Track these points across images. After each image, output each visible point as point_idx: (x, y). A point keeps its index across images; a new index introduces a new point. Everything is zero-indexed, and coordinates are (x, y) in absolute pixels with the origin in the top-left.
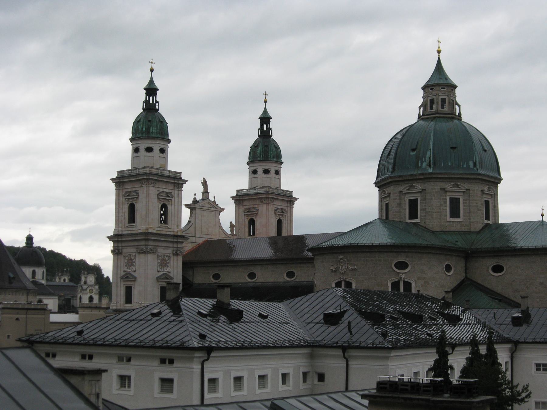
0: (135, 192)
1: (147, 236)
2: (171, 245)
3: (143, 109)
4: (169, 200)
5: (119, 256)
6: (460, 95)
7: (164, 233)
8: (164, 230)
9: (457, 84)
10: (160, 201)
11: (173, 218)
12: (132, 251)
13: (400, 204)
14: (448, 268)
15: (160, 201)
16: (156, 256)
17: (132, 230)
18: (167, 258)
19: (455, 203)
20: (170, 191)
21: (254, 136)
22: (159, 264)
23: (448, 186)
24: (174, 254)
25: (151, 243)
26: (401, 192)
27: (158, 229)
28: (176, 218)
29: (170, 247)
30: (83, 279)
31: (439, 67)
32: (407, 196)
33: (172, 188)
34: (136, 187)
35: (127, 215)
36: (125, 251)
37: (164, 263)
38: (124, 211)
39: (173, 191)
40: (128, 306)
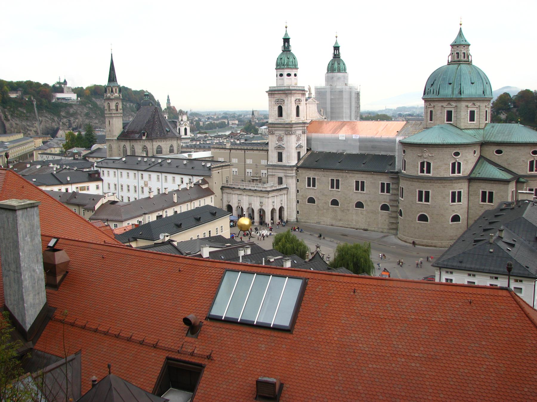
0: (282, 99)
1: (290, 125)
2: (301, 128)
3: (283, 51)
6: (472, 50)
7: (298, 122)
9: (470, 43)
12: (282, 133)
13: (441, 113)
14: (475, 152)
19: (472, 114)
21: (331, 57)
23: (470, 104)
24: (303, 133)
25: (293, 129)
26: (442, 106)
30: (180, 118)
31: (460, 33)
32: (446, 108)
33: (301, 96)
34: (283, 97)
35: (277, 112)
36: (276, 132)
37: (298, 139)
40: (280, 163)
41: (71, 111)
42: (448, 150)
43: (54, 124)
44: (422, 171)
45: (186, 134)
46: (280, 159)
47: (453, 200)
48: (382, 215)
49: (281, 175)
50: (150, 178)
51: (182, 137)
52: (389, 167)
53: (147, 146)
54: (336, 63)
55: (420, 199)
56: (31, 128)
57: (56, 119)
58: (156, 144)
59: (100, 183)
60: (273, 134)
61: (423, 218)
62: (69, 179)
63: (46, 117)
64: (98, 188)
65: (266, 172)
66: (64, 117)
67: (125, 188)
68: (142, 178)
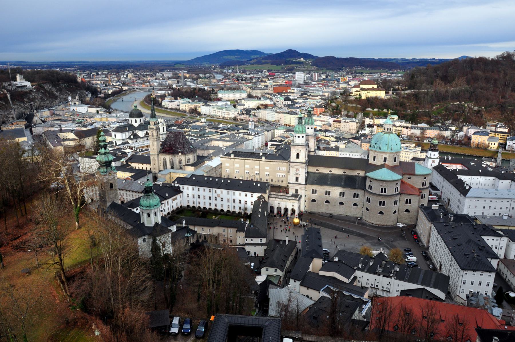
12: (299, 167)
17: (298, 160)
36: (295, 166)
40: (297, 182)
41: (31, 96)
42: (394, 182)
43: (22, 109)
44: (382, 192)
45: (164, 131)
46: (297, 179)
47: (395, 205)
48: (353, 208)
49: (297, 188)
50: (222, 192)
51: (161, 133)
52: (357, 185)
53: (182, 159)
54: (310, 120)
55: (380, 204)
56: (10, 116)
57: (22, 105)
58: (187, 157)
59: (181, 194)
60: (293, 167)
61: (381, 213)
62: (167, 195)
63: (17, 105)
64: (181, 197)
65: (258, 172)
66: (27, 102)
67: (202, 197)
68: (216, 192)
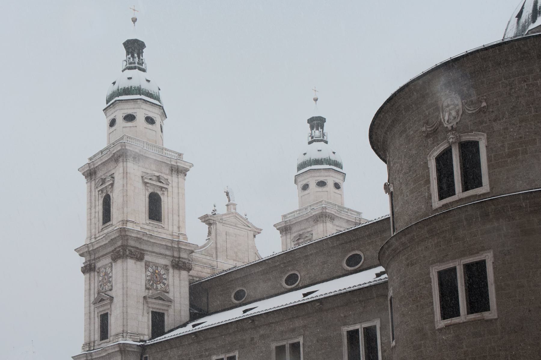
4: (163, 189)
5: (92, 274)
8: (156, 230)
10: (148, 187)
11: (170, 215)
15: (148, 187)
16: (143, 264)
18: (162, 272)
20: (166, 177)
22: (148, 278)
27: (146, 227)
28: (176, 217)
29: (166, 255)
38: (97, 210)
39: (169, 177)
